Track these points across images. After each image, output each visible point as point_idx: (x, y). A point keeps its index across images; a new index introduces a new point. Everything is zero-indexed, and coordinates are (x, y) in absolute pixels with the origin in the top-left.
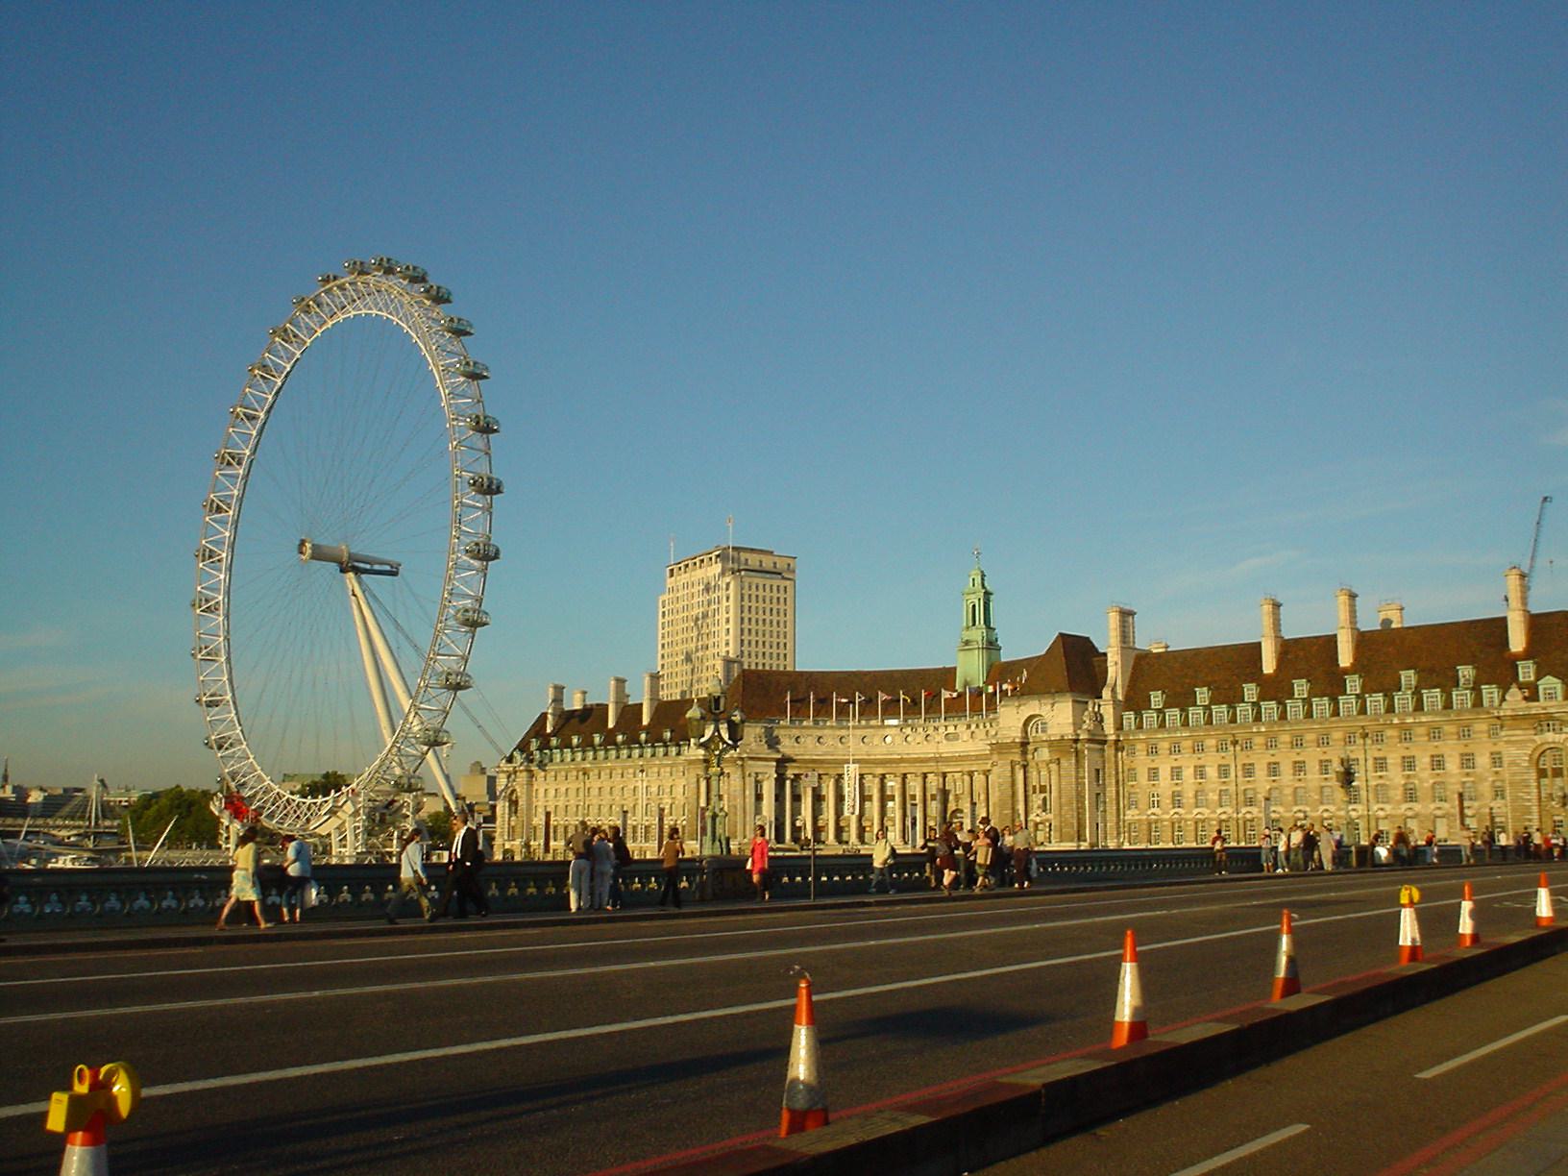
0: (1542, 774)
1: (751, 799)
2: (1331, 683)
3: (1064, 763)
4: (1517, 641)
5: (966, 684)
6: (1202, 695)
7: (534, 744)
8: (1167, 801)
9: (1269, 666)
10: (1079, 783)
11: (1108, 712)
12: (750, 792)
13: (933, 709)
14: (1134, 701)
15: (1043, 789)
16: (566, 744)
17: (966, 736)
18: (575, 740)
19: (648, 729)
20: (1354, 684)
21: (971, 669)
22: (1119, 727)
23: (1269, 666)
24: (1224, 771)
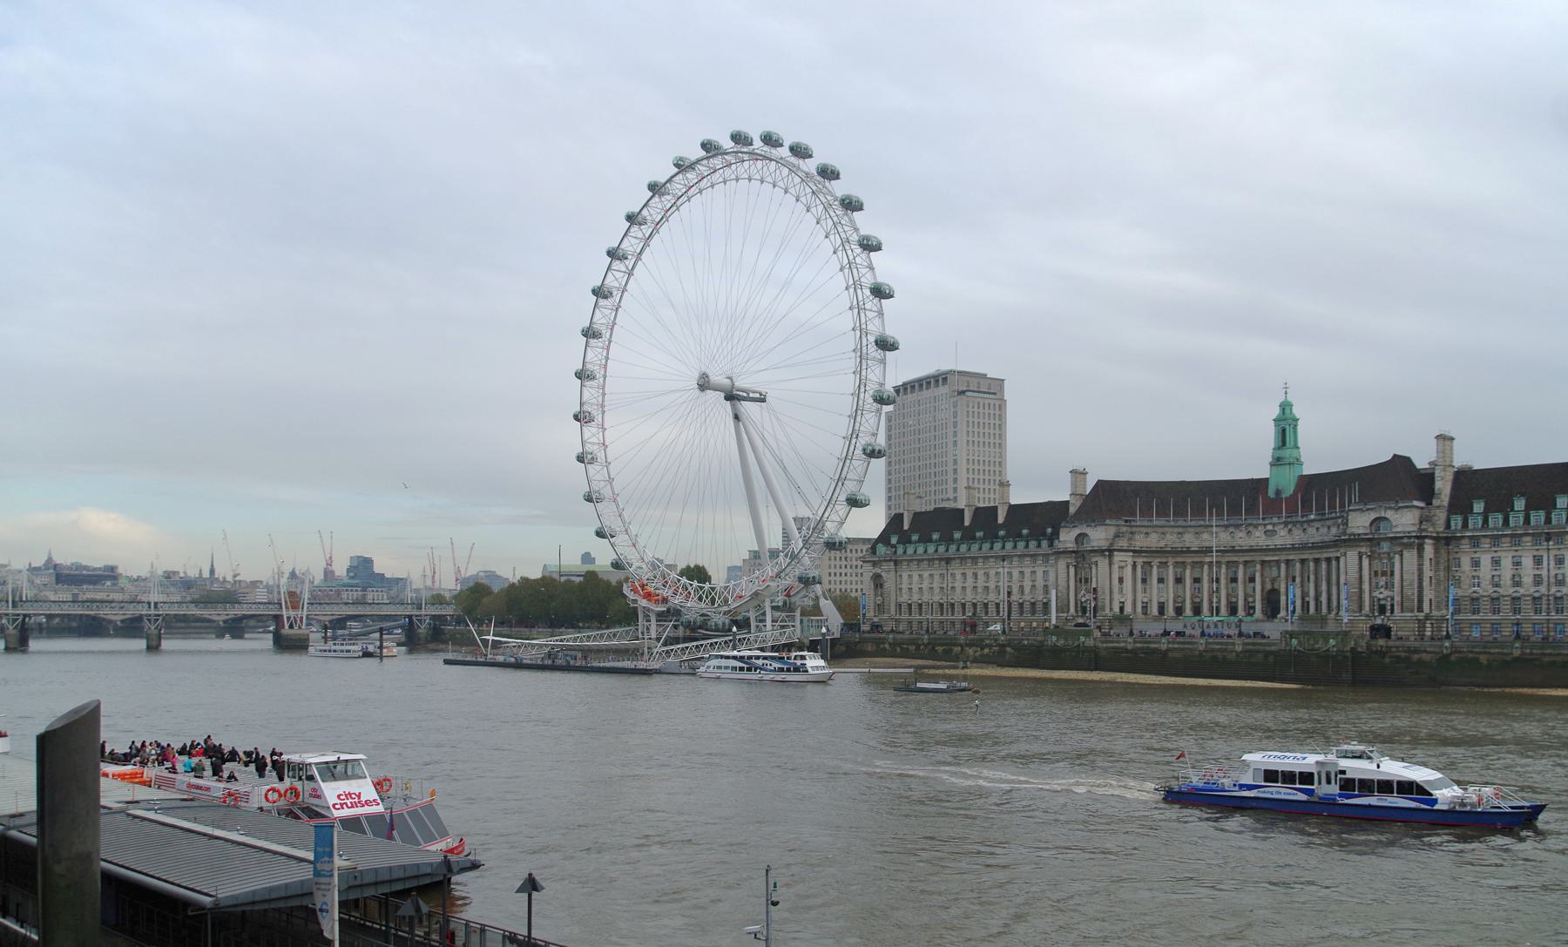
1: (1116, 581)
3: (1406, 554)
5: (1278, 492)
6: (1520, 504)
7: (894, 540)
11: (1441, 516)
12: (1116, 577)
13: (1252, 510)
14: (1459, 504)
15: (1384, 574)
16: (926, 539)
17: (1282, 532)
18: (935, 536)
21: (1286, 482)
22: (1448, 526)
24: (1538, 561)
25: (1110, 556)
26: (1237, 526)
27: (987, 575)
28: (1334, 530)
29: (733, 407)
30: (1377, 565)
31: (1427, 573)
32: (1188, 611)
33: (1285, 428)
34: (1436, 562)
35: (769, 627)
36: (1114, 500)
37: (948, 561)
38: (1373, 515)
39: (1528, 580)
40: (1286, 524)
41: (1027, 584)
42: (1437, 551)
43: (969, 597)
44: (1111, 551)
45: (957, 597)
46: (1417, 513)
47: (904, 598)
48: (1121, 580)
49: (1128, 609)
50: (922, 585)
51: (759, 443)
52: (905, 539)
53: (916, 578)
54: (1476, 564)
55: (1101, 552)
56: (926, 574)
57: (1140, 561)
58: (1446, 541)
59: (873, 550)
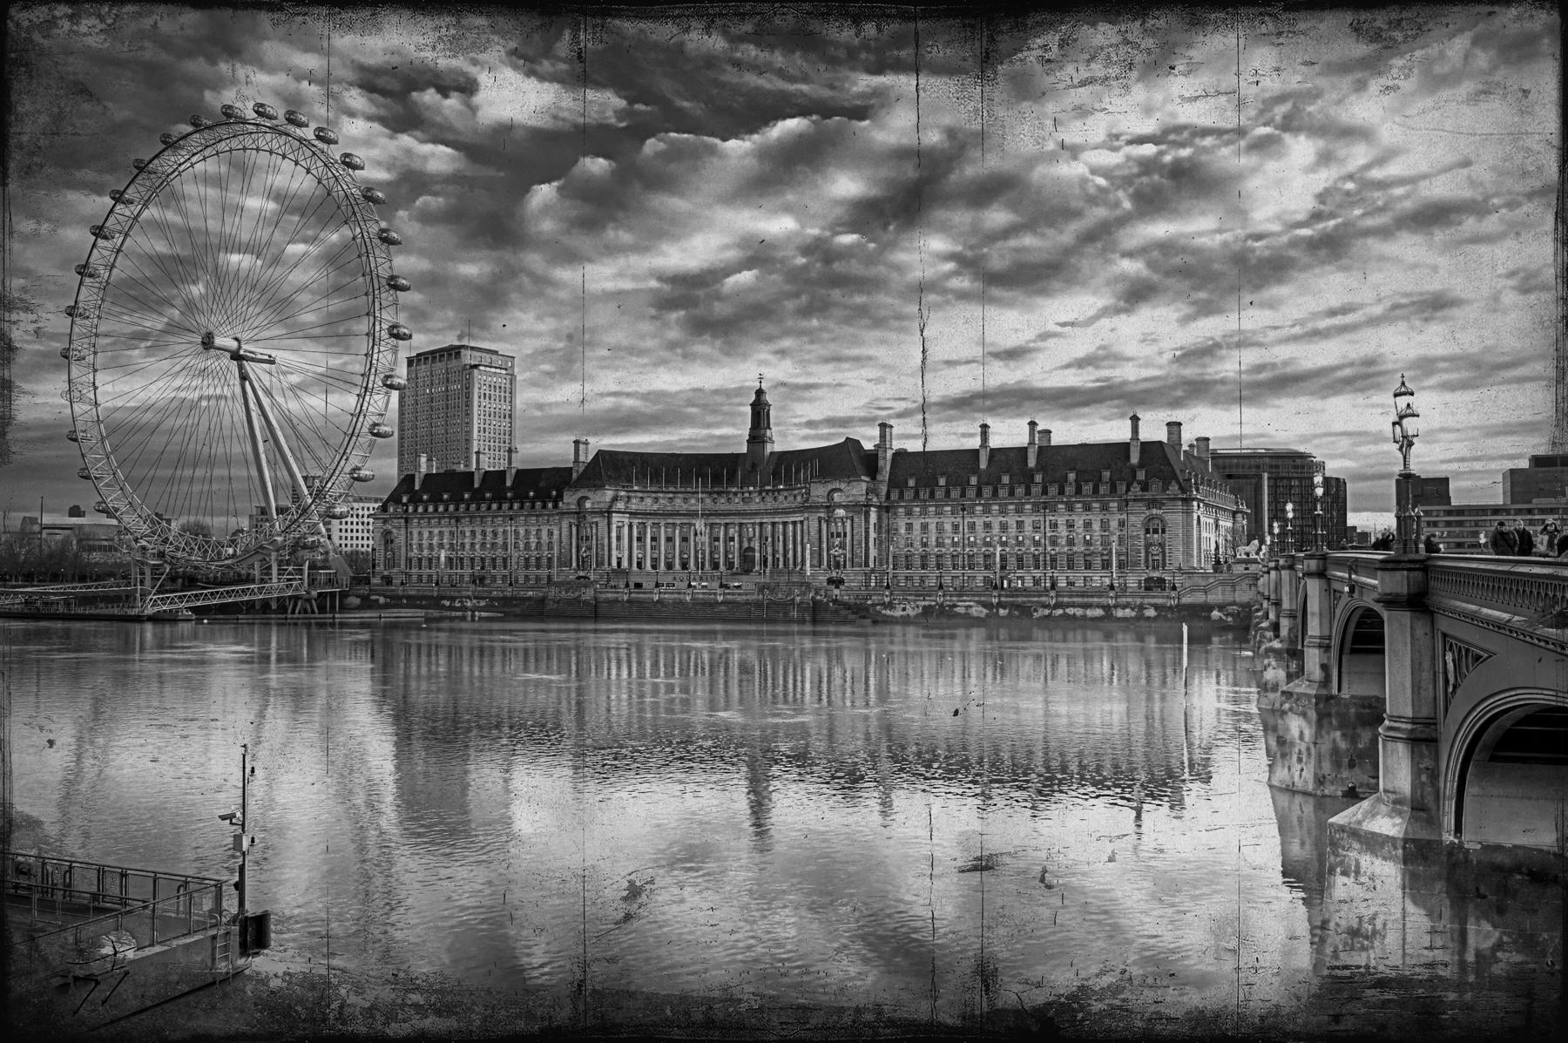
0: (1147, 531)
1: (614, 540)
2: (1026, 477)
4: (1135, 459)
7: (405, 500)
8: (917, 544)
9: (983, 465)
10: (867, 532)
11: (884, 489)
12: (614, 534)
13: (731, 480)
14: (896, 483)
15: (839, 535)
16: (436, 500)
19: (512, 488)
20: (1038, 478)
22: (888, 496)
23: (983, 465)
25: (609, 518)
26: (719, 493)
27: (495, 534)
28: (799, 498)
29: (241, 368)
30: (833, 529)
31: (872, 535)
32: (677, 566)
33: (760, 411)
34: (879, 527)
35: (275, 580)
36: (614, 468)
37: (458, 520)
38: (830, 487)
39: (948, 541)
40: (760, 493)
41: (533, 540)
42: (879, 518)
43: (478, 553)
44: (609, 513)
45: (466, 553)
46: (864, 486)
47: (415, 552)
48: (619, 538)
49: (625, 564)
50: (434, 541)
51: (265, 401)
52: (415, 499)
53: (426, 535)
54: (909, 527)
55: (601, 513)
56: (436, 531)
57: (635, 521)
58: (886, 509)
59: (384, 508)
